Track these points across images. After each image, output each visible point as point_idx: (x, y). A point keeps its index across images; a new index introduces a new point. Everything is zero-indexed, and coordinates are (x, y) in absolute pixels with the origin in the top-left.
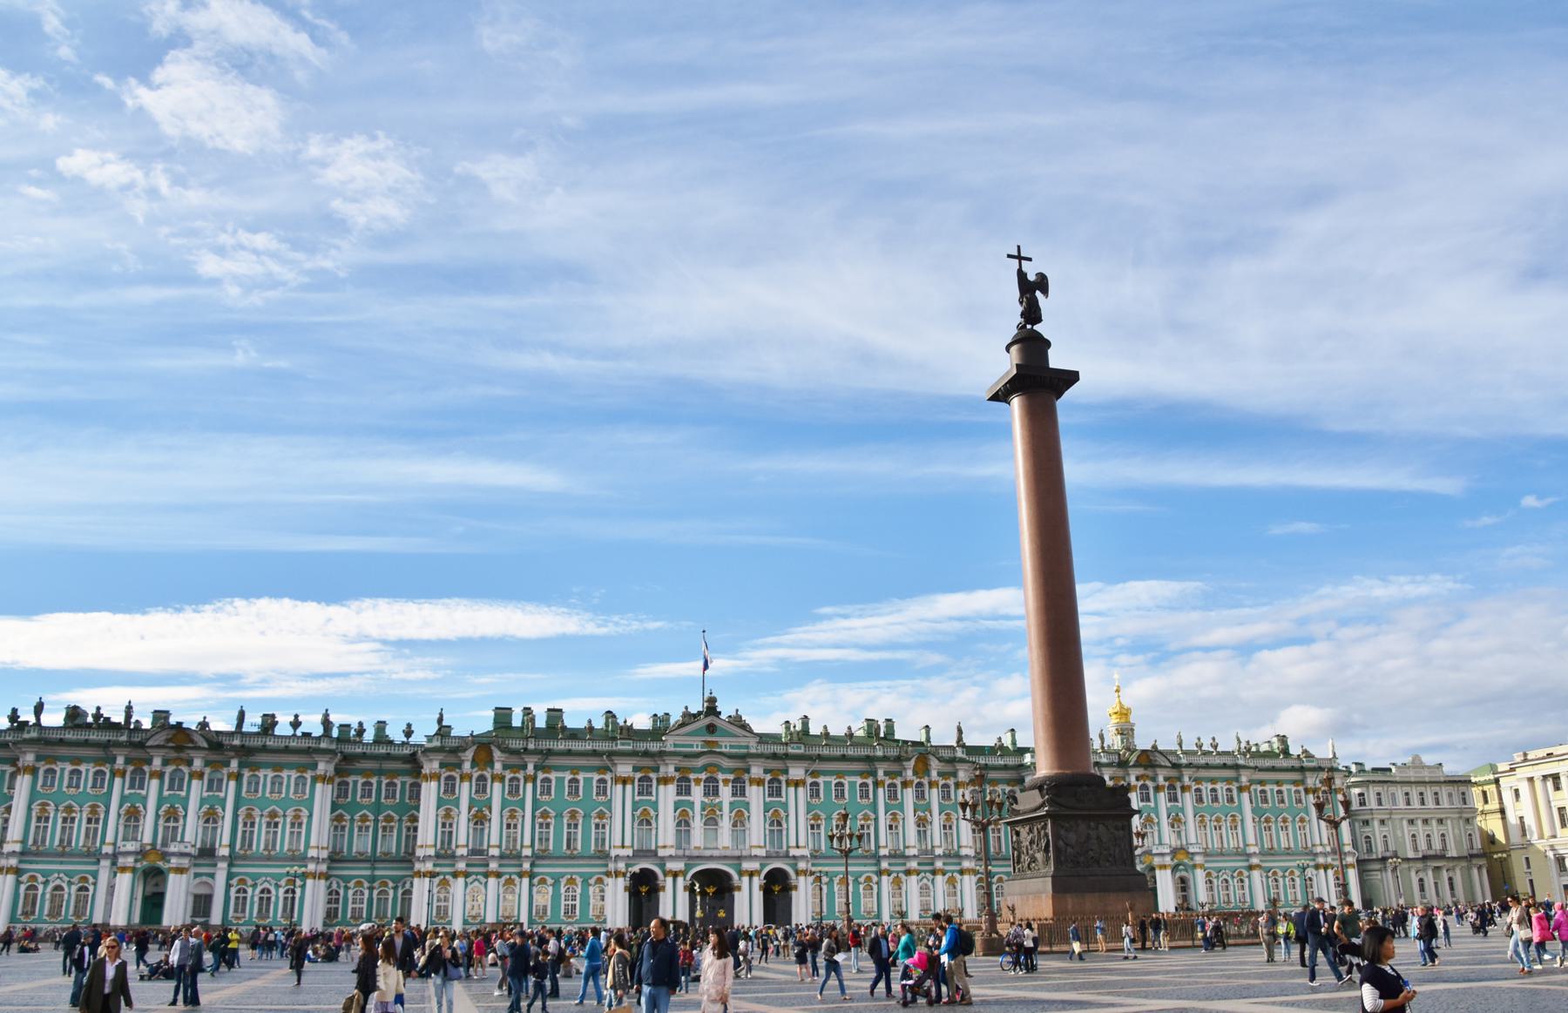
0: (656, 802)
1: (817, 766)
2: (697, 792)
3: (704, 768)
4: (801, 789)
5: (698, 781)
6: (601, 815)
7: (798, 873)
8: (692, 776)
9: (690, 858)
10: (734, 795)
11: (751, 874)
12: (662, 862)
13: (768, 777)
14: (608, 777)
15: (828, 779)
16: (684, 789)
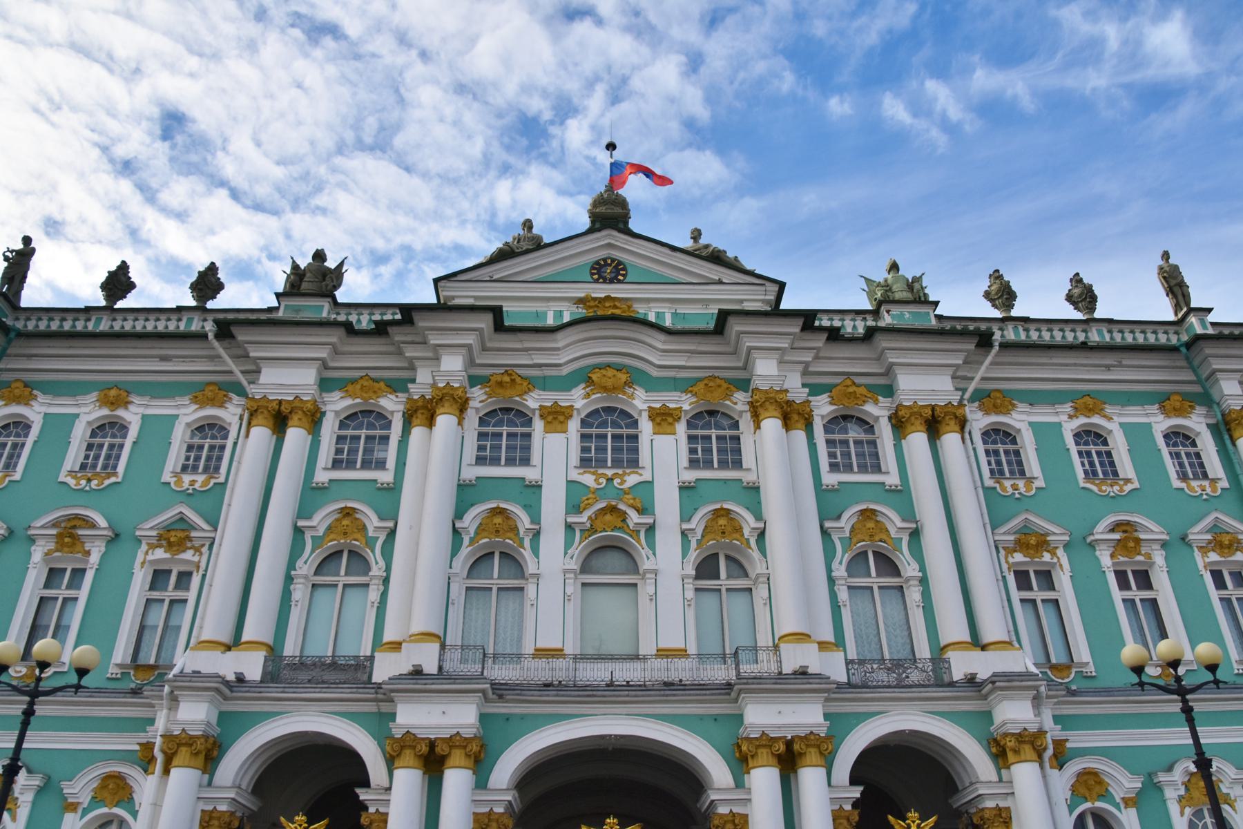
0: (394, 489)
1: (986, 369)
2: (555, 457)
3: (585, 377)
4: (951, 441)
5: (556, 417)
6: (176, 536)
7: (1001, 753)
8: (533, 401)
9: (500, 691)
10: (694, 464)
11: (789, 758)
12: (378, 703)
13: (823, 408)
14: (231, 414)
15: (1044, 415)
16: (506, 431)
